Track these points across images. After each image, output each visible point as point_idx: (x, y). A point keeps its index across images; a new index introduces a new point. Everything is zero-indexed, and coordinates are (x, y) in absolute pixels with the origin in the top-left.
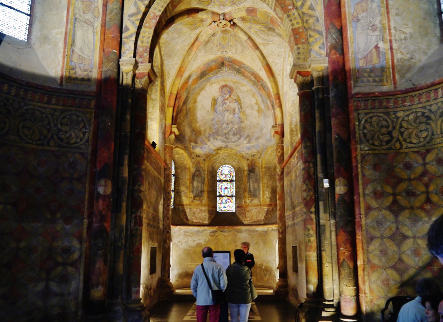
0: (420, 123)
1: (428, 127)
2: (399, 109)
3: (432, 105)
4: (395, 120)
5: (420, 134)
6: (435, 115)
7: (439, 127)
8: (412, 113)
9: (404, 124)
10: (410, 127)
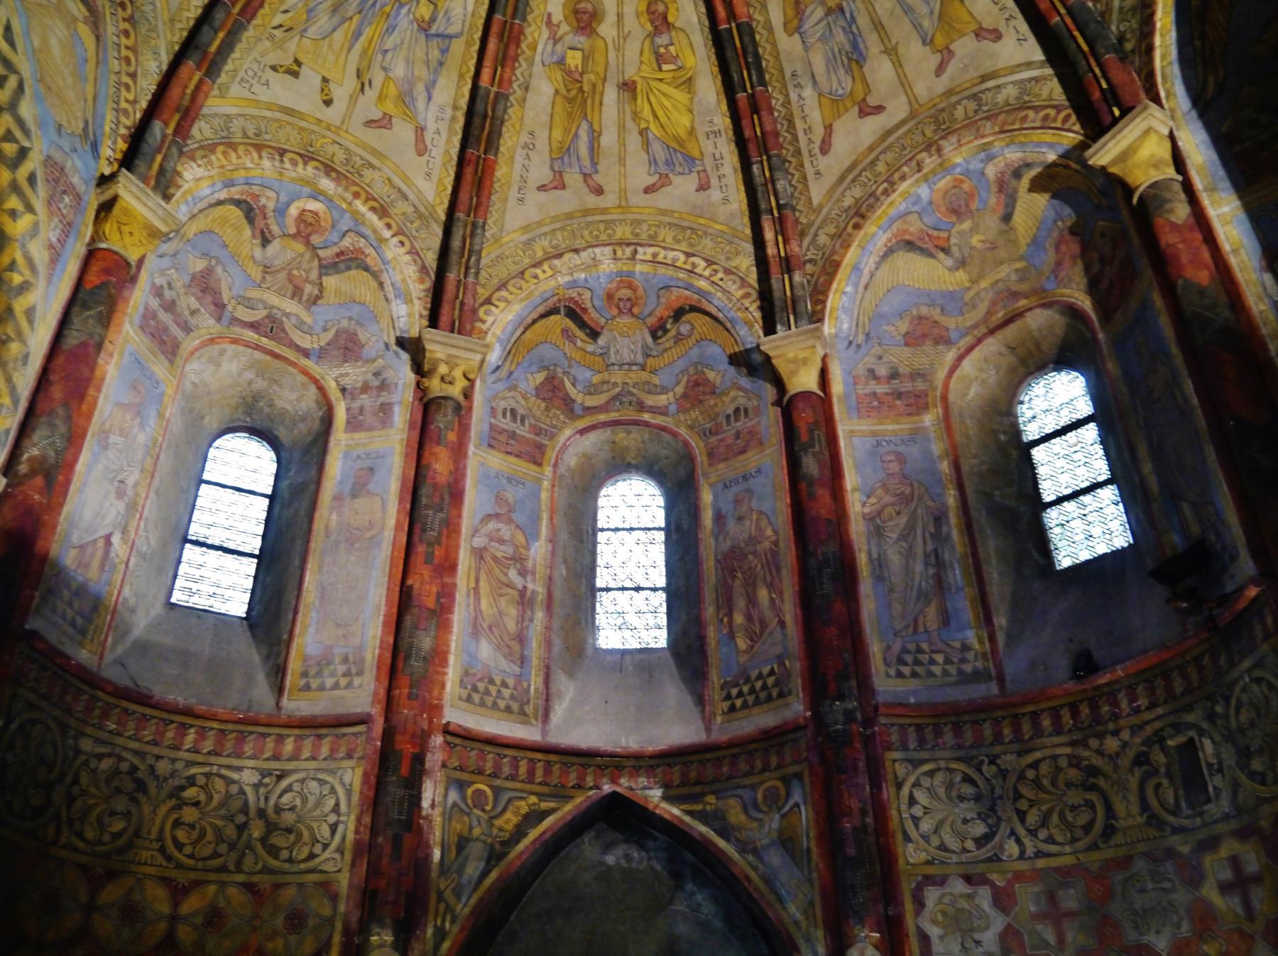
0: (118, 790)
1: (134, 810)
2: (88, 730)
3: (162, 757)
4: (71, 754)
5: (107, 820)
6: (159, 787)
7: (158, 821)
8: (110, 755)
9: (84, 778)
10: (93, 790)
